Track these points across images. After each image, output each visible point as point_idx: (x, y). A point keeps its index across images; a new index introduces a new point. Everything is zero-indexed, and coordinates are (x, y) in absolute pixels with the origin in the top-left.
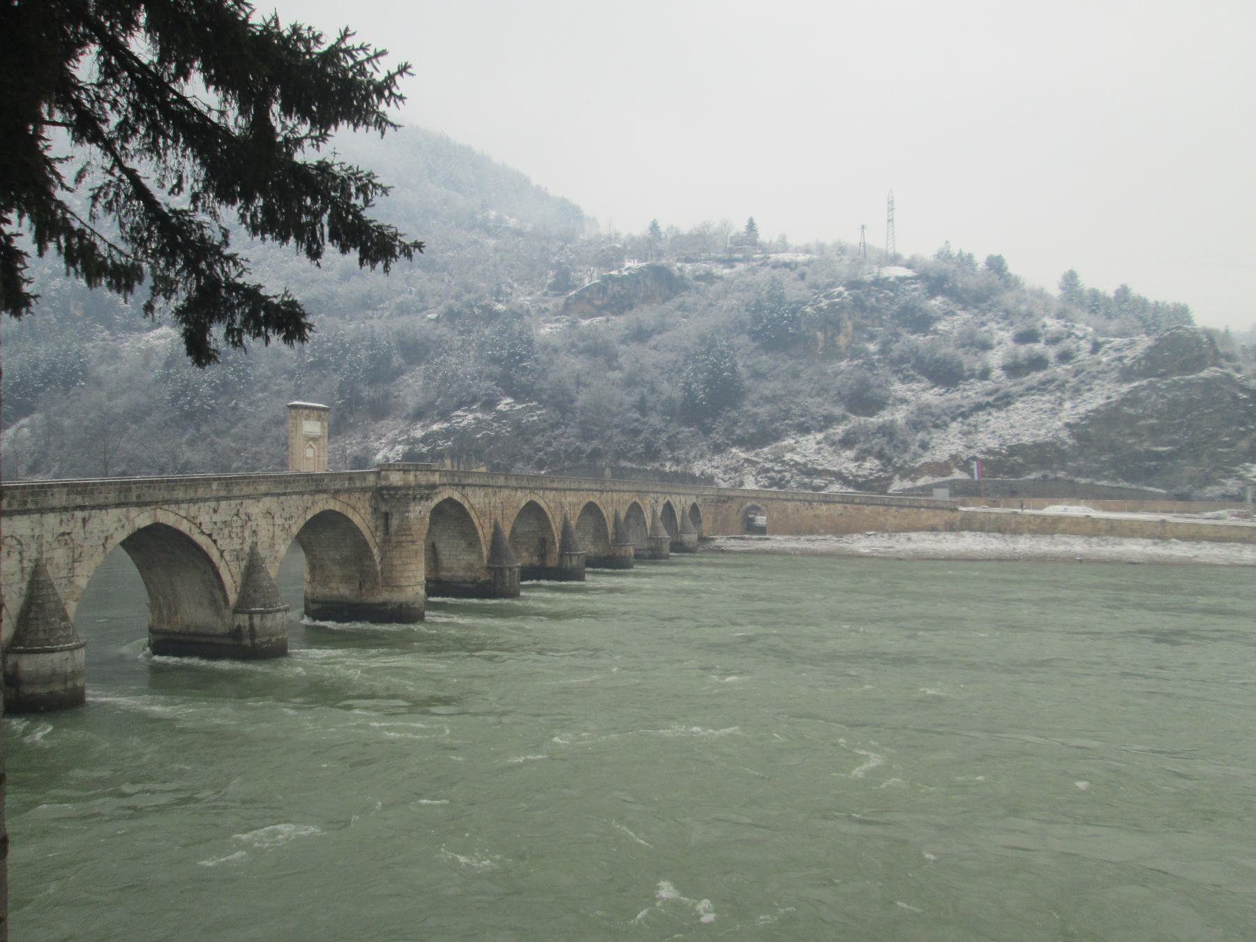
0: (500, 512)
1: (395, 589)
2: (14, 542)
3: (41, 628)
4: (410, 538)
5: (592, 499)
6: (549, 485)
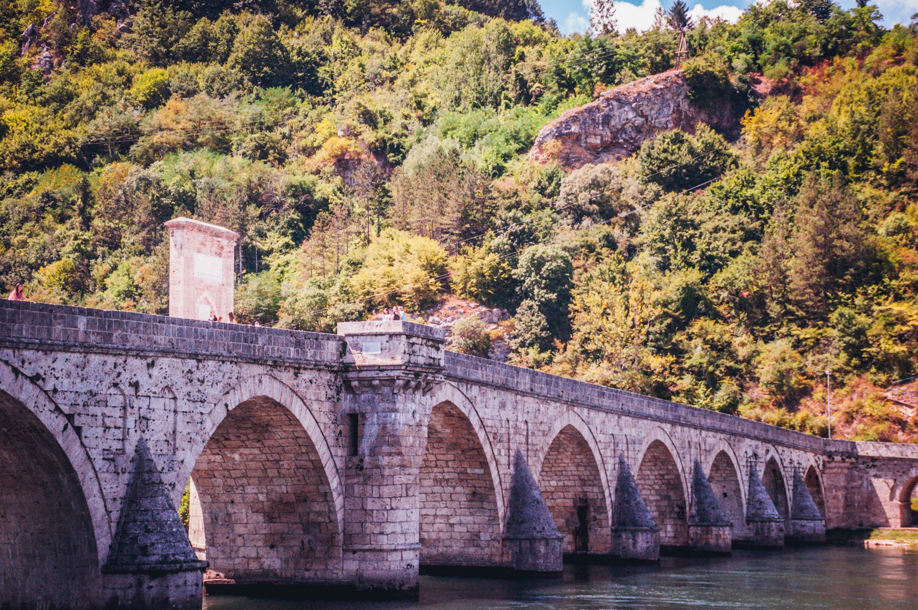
0: (524, 440)
1: (369, 555)
4: (396, 460)
6: (596, 402)
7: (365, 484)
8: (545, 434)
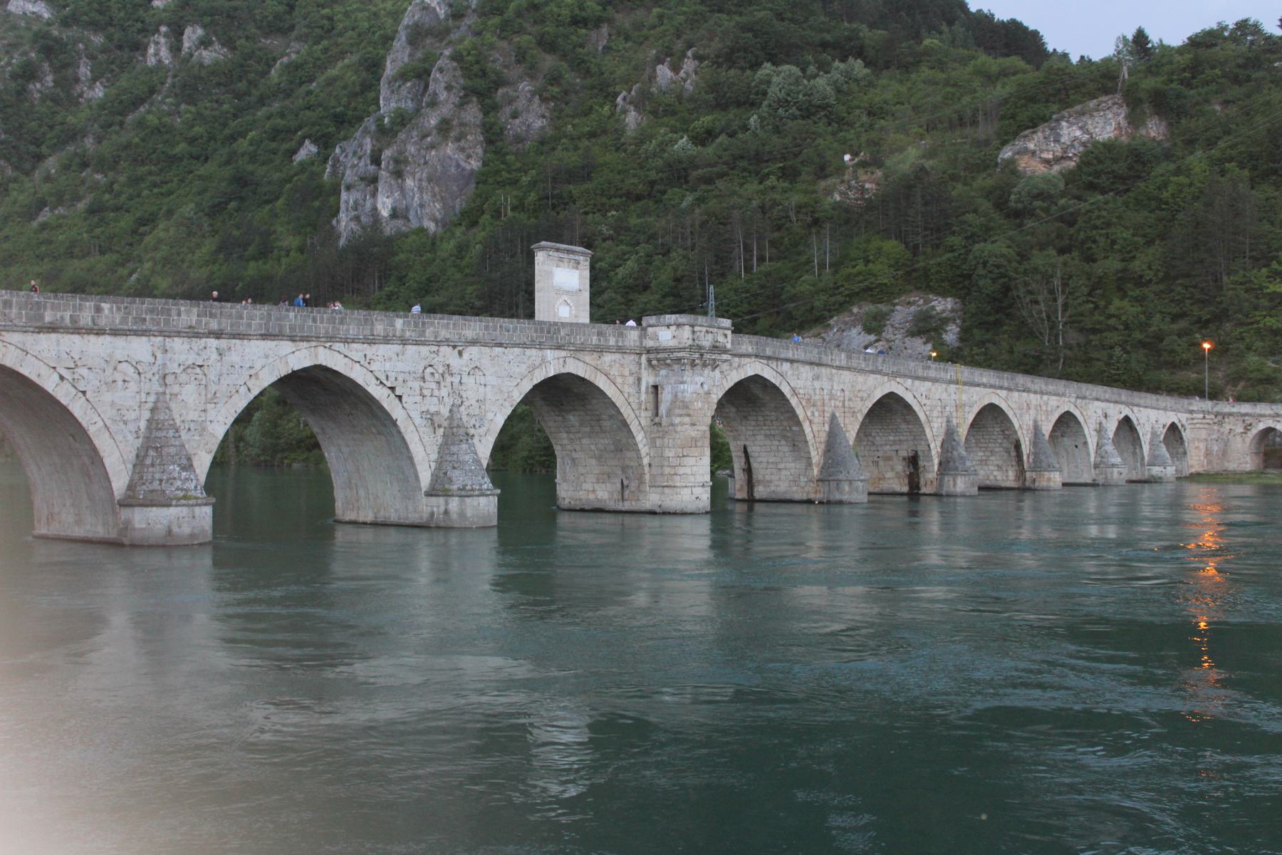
0: (841, 404)
1: (666, 490)
2: (132, 370)
3: (157, 476)
4: (687, 420)
6: (920, 374)
7: (663, 438)
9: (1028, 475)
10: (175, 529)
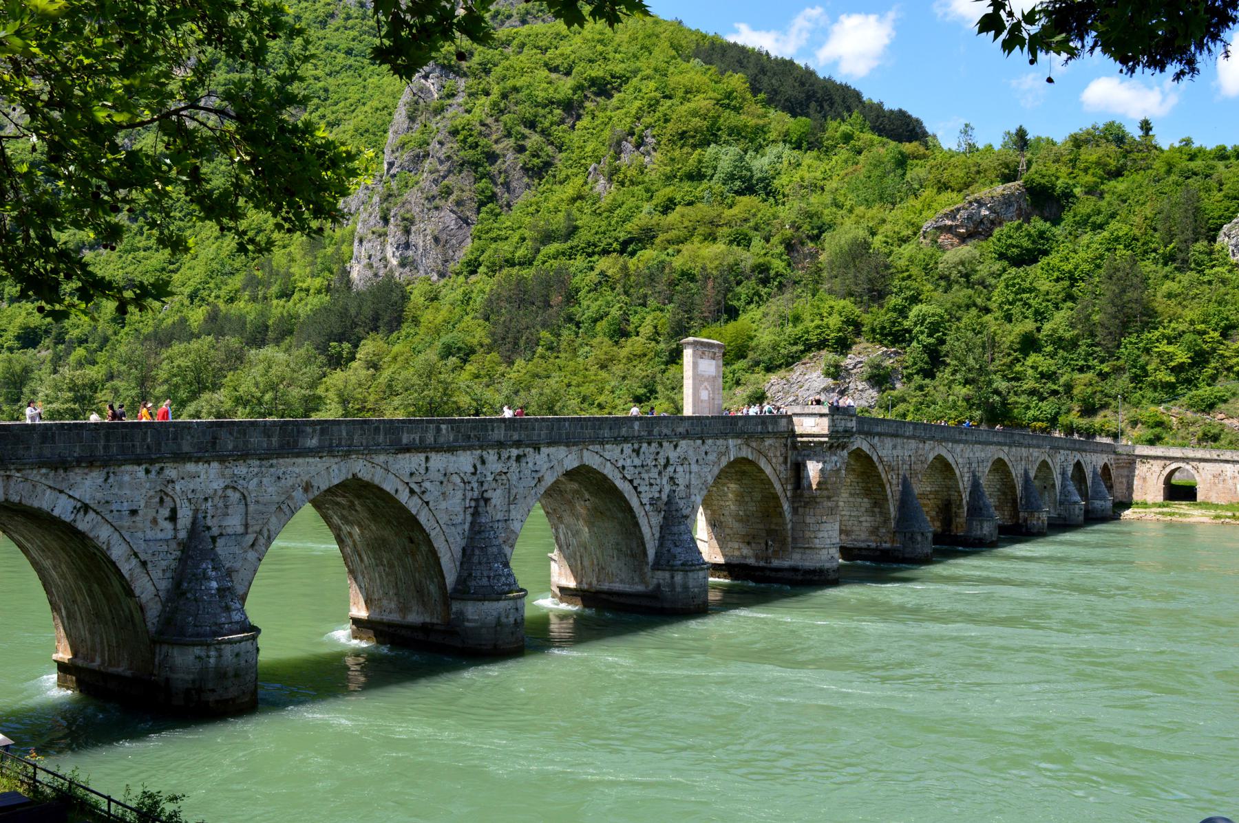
0: (908, 467)
1: (807, 551)
4: (825, 493)
5: (1002, 455)
8: (922, 462)
9: (1021, 514)
10: (504, 620)
